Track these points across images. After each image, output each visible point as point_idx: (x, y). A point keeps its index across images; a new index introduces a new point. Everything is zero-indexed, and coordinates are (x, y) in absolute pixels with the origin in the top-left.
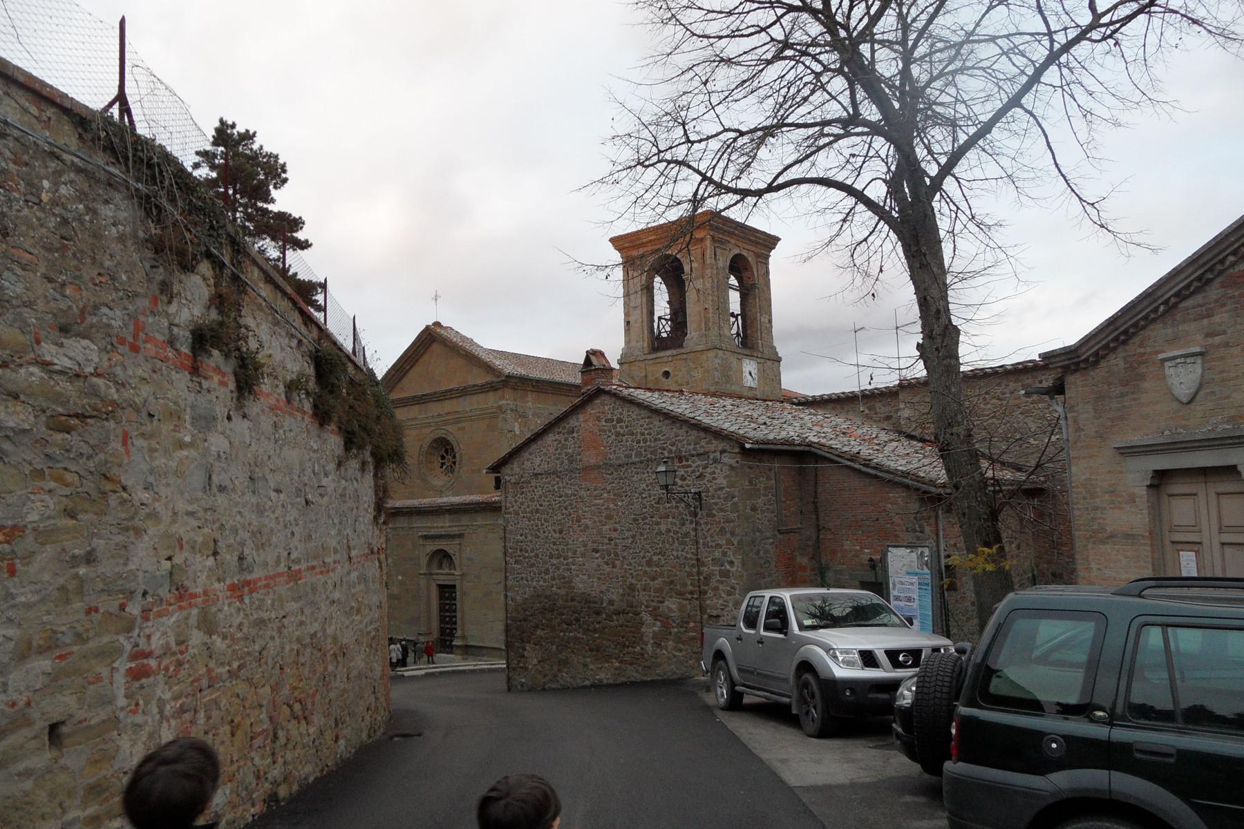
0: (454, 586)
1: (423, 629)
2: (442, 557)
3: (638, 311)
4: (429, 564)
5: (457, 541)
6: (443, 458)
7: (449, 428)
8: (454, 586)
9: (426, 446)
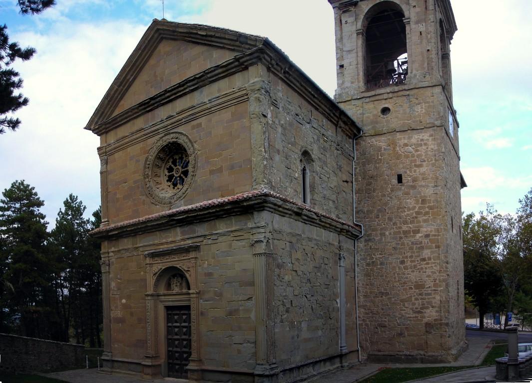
0: (188, 308)
1: (151, 352)
2: (174, 275)
5: (192, 255)
6: (170, 170)
8: (188, 308)
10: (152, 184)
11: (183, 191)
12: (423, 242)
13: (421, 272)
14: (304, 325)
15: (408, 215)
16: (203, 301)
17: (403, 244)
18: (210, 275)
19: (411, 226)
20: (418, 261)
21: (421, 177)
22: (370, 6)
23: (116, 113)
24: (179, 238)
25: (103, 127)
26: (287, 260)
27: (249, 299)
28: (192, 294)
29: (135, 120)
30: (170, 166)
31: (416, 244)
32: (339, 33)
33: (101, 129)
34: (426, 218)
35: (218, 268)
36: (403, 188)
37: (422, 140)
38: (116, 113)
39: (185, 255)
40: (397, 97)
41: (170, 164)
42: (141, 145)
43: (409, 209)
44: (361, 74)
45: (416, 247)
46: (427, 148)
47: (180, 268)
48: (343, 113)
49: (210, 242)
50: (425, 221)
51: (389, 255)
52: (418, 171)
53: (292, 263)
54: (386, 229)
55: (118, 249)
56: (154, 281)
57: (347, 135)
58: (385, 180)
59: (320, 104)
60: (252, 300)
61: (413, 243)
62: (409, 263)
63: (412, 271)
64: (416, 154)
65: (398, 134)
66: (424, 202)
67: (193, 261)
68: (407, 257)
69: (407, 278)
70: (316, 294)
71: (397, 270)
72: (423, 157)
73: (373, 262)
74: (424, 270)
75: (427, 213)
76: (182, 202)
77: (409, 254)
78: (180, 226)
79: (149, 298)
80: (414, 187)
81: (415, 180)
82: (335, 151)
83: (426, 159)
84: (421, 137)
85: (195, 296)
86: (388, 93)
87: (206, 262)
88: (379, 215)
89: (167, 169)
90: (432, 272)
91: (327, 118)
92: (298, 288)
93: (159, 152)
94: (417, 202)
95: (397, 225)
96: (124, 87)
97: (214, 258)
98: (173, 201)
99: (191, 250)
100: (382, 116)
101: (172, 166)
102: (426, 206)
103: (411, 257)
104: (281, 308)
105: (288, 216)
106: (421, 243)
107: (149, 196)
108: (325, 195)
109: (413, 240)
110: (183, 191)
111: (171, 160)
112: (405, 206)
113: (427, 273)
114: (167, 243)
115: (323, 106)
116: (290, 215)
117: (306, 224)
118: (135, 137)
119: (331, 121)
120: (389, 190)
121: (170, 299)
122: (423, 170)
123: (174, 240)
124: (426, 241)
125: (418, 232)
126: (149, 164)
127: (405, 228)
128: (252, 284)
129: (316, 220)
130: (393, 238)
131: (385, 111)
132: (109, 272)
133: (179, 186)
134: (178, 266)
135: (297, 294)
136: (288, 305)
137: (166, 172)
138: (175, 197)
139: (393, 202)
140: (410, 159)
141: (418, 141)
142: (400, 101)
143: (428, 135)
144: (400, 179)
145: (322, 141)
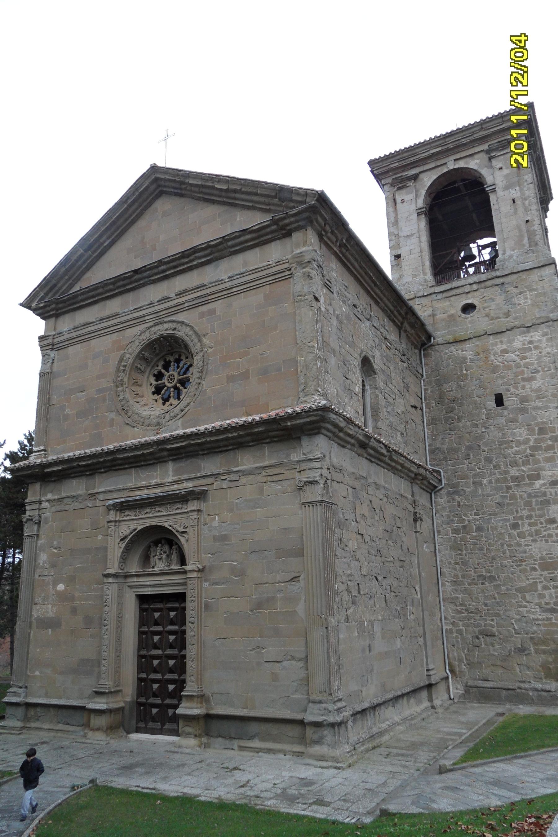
0: (182, 597)
2: (159, 540)
3: (414, 240)
4: (124, 558)
5: (193, 505)
6: (159, 376)
7: (180, 317)
8: (182, 597)
9: (130, 358)
10: (127, 395)
11: (181, 406)
12: (548, 493)
13: (549, 541)
14: (377, 628)
16: (210, 585)
17: (513, 497)
18: (224, 538)
19: (524, 469)
20: (541, 523)
21: (534, 395)
22: (435, 177)
23: (76, 288)
24: (170, 479)
25: (53, 306)
26: (350, 516)
27: (292, 580)
28: (190, 571)
30: (160, 372)
32: (392, 215)
33: (48, 309)
34: (550, 455)
35: (237, 526)
36: (506, 413)
37: (530, 342)
38: (76, 288)
39: (180, 506)
40: (485, 288)
41: (160, 368)
42: (114, 336)
43: (519, 443)
44: (428, 263)
45: (537, 501)
46: (540, 353)
47: (170, 528)
48: (411, 311)
49: (225, 484)
50: (549, 460)
51: (490, 515)
52: (528, 386)
53: (356, 520)
54: (482, 475)
55: (59, 497)
56: (121, 550)
57: (413, 343)
58: (475, 403)
59: (381, 295)
60: (299, 581)
61: (530, 495)
62: (527, 528)
63: (533, 541)
65: (491, 337)
66: (542, 431)
67: (194, 516)
68: (521, 518)
69: (525, 552)
70: (389, 575)
71: (507, 540)
72: (535, 367)
73: (464, 527)
75: (550, 448)
76: (180, 422)
77: (525, 513)
78: (173, 460)
79: (110, 580)
80: (524, 411)
81: (524, 400)
82: (400, 363)
83: (539, 369)
84: (528, 339)
85: (195, 575)
86: (470, 284)
88: (469, 455)
89: (155, 375)
91: (389, 317)
92: (366, 564)
93: (142, 350)
94: (531, 431)
95: (500, 468)
97: (231, 511)
98: (163, 421)
99: (190, 498)
100: (463, 315)
101: (163, 371)
102: (548, 436)
103: (529, 517)
104: (346, 597)
105: (349, 446)
106: (544, 494)
107: (122, 413)
108: (392, 423)
109: (529, 490)
110: (181, 406)
111: (161, 363)
112: (511, 439)
114: (148, 487)
115: (385, 299)
116: (353, 445)
117: (372, 462)
118: (105, 325)
119: (393, 321)
120: (484, 417)
121: (148, 583)
122: (535, 384)
123: (162, 481)
125: (538, 477)
126: (125, 366)
127: (514, 472)
128: (300, 553)
129: (385, 456)
130: (495, 489)
131: (468, 308)
132: (38, 535)
133: (172, 400)
134: (166, 525)
135: (365, 573)
136: (355, 593)
137: (152, 380)
138: (167, 415)
139: (491, 434)
140: (514, 370)
141: (524, 344)
142: (489, 293)
143: (540, 333)
144: (499, 400)
145: (384, 346)
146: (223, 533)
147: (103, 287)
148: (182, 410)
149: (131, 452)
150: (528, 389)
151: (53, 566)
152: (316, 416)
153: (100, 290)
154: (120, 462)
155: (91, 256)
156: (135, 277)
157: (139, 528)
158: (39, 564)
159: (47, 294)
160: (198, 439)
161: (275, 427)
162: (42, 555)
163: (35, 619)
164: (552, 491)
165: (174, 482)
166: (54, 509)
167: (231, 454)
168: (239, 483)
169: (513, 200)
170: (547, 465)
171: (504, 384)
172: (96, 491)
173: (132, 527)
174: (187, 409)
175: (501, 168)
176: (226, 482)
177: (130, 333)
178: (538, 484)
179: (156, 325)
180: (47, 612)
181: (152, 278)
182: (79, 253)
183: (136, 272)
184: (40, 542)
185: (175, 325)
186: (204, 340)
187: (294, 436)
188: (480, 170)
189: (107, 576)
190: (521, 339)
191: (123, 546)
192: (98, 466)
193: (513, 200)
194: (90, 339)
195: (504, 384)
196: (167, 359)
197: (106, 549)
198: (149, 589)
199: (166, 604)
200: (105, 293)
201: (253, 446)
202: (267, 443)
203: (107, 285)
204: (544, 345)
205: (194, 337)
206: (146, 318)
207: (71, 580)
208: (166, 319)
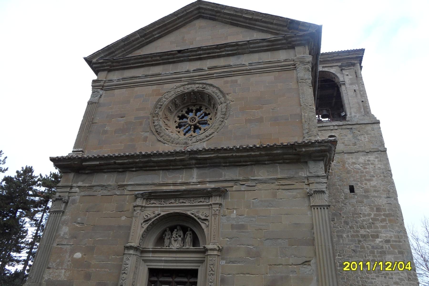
0: (194, 273)
8: (194, 273)
10: (161, 123)
12: (384, 247)
13: (387, 277)
15: (364, 220)
16: (226, 263)
19: (369, 231)
21: (372, 189)
24: (195, 180)
28: (211, 250)
29: (151, 67)
31: (376, 248)
34: (384, 224)
35: (254, 219)
36: (356, 197)
37: (369, 161)
39: (203, 200)
40: (342, 129)
43: (365, 215)
45: (378, 251)
46: (375, 167)
49: (243, 188)
50: (383, 227)
51: (348, 257)
52: (368, 184)
58: (337, 189)
60: (310, 265)
61: (373, 247)
63: (376, 276)
64: (364, 171)
65: (346, 155)
66: (378, 210)
67: (216, 208)
69: (372, 283)
71: (360, 274)
72: (372, 174)
74: (390, 276)
75: (383, 220)
78: (197, 168)
80: (367, 197)
81: (366, 191)
83: (375, 175)
85: (215, 253)
86: (334, 126)
87: (235, 212)
88: (334, 219)
89: (178, 117)
90: (399, 279)
94: (372, 209)
95: (354, 229)
96: (146, 39)
98: (190, 142)
99: (214, 194)
102: (382, 213)
106: (382, 247)
107: (156, 133)
109: (372, 244)
112: (360, 212)
113: (394, 279)
114: (174, 184)
120: (343, 197)
122: (373, 183)
123: (188, 181)
124: (387, 246)
125: (377, 237)
126: (162, 105)
127: (362, 232)
139: (347, 208)
140: (360, 174)
141: (365, 161)
142: (344, 132)
143: (374, 157)
144: (352, 189)
146: (240, 223)
147: (152, 57)
148: (207, 137)
149: (165, 157)
150: (368, 185)
151: (74, 237)
152: (326, 146)
153: (149, 59)
154: (152, 164)
155: (143, 41)
156: (178, 55)
157: (162, 214)
158: (60, 235)
159: (106, 56)
160: (226, 153)
161: (291, 151)
162: (64, 228)
163: (46, 281)
164: (386, 246)
165: (199, 182)
166: (83, 194)
167: (249, 168)
168: (255, 188)
169: (355, 90)
170: (383, 230)
171: (354, 180)
172: (125, 183)
173: (157, 213)
174: (211, 136)
175: (347, 75)
176: (244, 186)
177: (168, 87)
178: (378, 240)
179: (188, 84)
180: (59, 276)
181: (190, 58)
182: (137, 37)
183: (179, 51)
184: (64, 218)
185: (205, 86)
186: (228, 97)
187: (302, 160)
188: (336, 74)
189: (131, 248)
190: (363, 158)
191: (146, 226)
192: (131, 166)
193: (355, 90)
194: (134, 87)
195: (354, 180)
196: (194, 105)
197: (129, 228)
198: (163, 264)
199: (175, 278)
200: (152, 61)
201: (268, 164)
202: (279, 163)
203: (155, 56)
204: (376, 163)
205: (219, 94)
206: (183, 79)
207: (89, 250)
208: (197, 82)
